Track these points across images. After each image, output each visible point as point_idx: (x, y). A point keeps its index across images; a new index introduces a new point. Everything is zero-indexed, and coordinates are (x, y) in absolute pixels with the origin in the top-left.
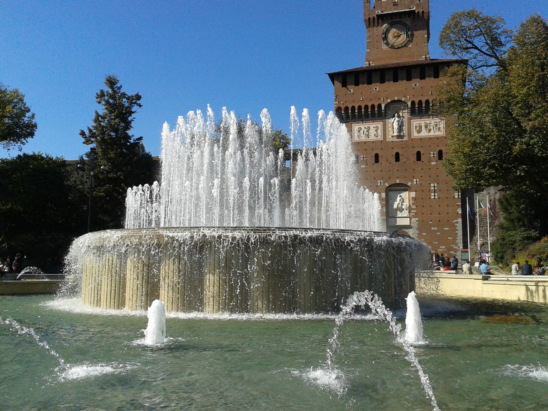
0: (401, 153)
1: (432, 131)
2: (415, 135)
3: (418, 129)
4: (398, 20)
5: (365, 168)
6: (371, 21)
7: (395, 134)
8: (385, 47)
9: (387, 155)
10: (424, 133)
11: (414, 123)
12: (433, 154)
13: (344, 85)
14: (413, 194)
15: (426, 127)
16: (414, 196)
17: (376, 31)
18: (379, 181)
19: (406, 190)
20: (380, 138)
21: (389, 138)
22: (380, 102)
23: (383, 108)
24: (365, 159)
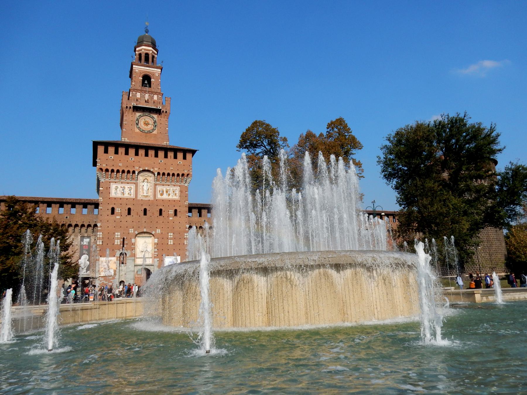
1: (171, 195)
2: (159, 197)
3: (161, 192)
5: (120, 219)
7: (145, 194)
8: (137, 130)
9: (137, 210)
10: (165, 196)
12: (172, 212)
13: (106, 151)
14: (156, 241)
15: (167, 192)
17: (131, 116)
18: (130, 230)
21: (140, 197)
22: (134, 170)
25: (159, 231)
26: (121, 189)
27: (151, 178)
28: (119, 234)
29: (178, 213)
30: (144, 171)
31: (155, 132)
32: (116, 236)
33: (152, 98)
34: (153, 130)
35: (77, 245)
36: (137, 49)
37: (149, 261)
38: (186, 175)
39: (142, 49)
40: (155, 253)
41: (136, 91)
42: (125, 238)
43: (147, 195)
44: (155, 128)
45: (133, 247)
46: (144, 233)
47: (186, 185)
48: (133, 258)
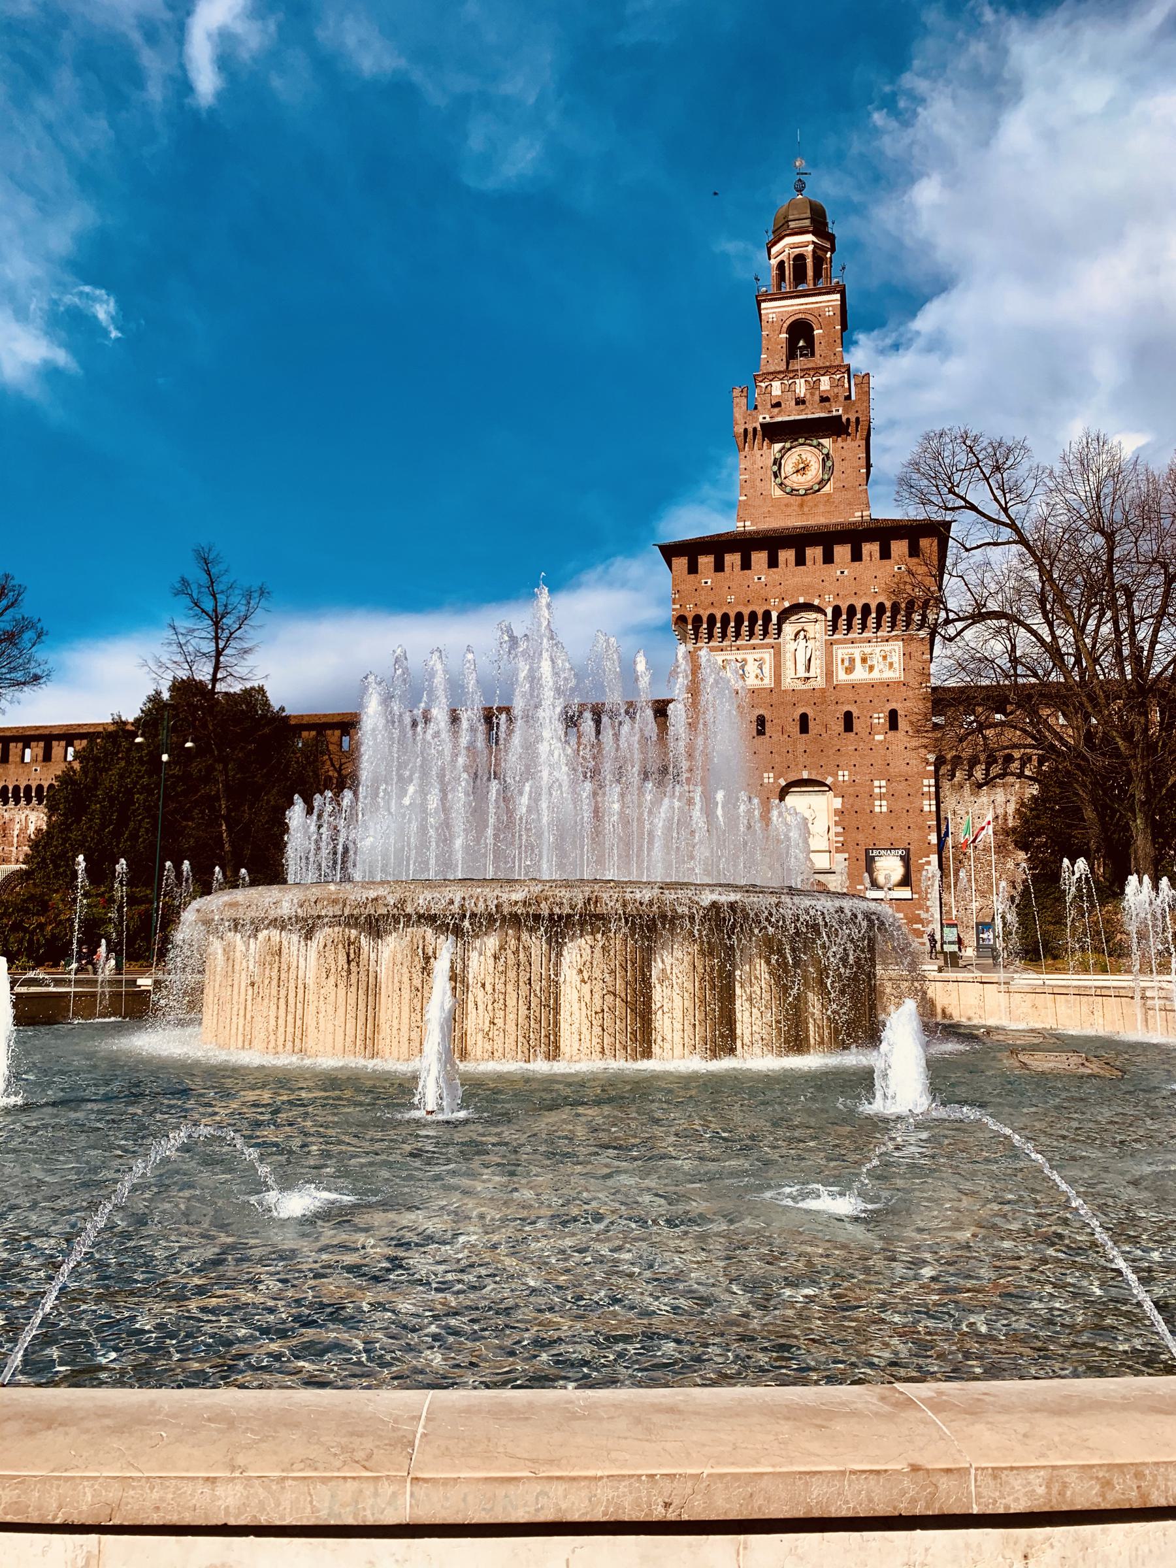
1: (876, 670)
2: (841, 676)
3: (847, 664)
6: (750, 436)
7: (802, 673)
8: (778, 492)
10: (860, 674)
11: (840, 651)
12: (880, 719)
14: (838, 803)
15: (864, 660)
16: (840, 806)
18: (766, 775)
20: (768, 682)
21: (788, 682)
23: (774, 619)
25: (843, 776)
31: (827, 489)
34: (822, 483)
36: (774, 250)
41: (771, 377)
43: (807, 675)
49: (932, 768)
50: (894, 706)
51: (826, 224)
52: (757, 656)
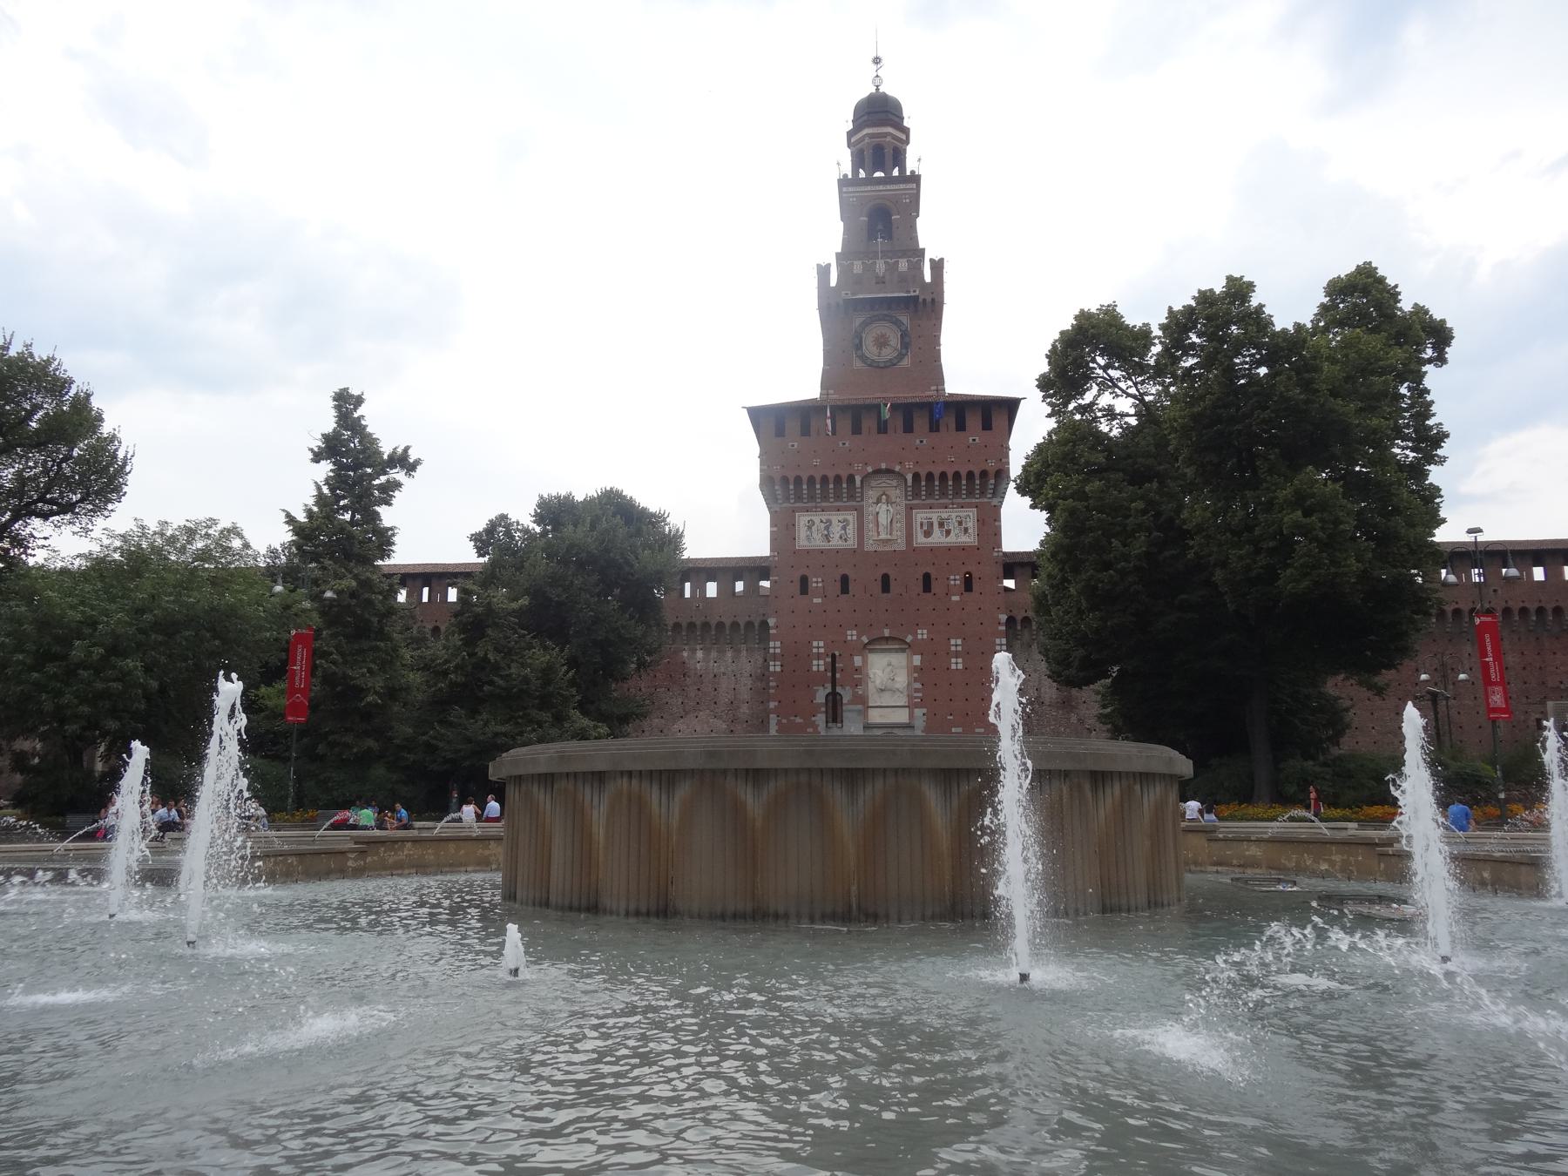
0: (892, 578)
2: (920, 540)
3: (925, 528)
4: (886, 312)
7: (883, 536)
10: (938, 538)
12: (956, 580)
15: (941, 525)
18: (849, 632)
19: (903, 650)
21: (870, 546)
22: (852, 472)
24: (820, 585)
25: (923, 634)
26: (823, 525)
27: (898, 491)
28: (821, 644)
29: (975, 586)
30: (878, 472)
31: (906, 362)
32: (815, 650)
33: (892, 268)
34: (901, 357)
35: (724, 674)
37: (902, 717)
38: (992, 473)
39: (864, 136)
40: (916, 695)
42: (837, 653)
43: (889, 537)
44: (904, 351)
45: (858, 678)
46: (887, 639)
47: (995, 502)
48: (860, 707)
49: (1004, 628)
50: (969, 569)
51: (902, 119)
52: (841, 518)
